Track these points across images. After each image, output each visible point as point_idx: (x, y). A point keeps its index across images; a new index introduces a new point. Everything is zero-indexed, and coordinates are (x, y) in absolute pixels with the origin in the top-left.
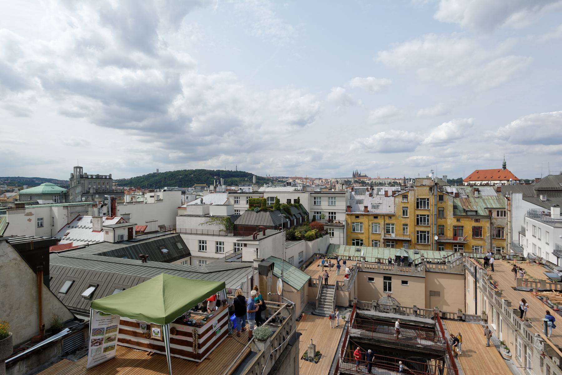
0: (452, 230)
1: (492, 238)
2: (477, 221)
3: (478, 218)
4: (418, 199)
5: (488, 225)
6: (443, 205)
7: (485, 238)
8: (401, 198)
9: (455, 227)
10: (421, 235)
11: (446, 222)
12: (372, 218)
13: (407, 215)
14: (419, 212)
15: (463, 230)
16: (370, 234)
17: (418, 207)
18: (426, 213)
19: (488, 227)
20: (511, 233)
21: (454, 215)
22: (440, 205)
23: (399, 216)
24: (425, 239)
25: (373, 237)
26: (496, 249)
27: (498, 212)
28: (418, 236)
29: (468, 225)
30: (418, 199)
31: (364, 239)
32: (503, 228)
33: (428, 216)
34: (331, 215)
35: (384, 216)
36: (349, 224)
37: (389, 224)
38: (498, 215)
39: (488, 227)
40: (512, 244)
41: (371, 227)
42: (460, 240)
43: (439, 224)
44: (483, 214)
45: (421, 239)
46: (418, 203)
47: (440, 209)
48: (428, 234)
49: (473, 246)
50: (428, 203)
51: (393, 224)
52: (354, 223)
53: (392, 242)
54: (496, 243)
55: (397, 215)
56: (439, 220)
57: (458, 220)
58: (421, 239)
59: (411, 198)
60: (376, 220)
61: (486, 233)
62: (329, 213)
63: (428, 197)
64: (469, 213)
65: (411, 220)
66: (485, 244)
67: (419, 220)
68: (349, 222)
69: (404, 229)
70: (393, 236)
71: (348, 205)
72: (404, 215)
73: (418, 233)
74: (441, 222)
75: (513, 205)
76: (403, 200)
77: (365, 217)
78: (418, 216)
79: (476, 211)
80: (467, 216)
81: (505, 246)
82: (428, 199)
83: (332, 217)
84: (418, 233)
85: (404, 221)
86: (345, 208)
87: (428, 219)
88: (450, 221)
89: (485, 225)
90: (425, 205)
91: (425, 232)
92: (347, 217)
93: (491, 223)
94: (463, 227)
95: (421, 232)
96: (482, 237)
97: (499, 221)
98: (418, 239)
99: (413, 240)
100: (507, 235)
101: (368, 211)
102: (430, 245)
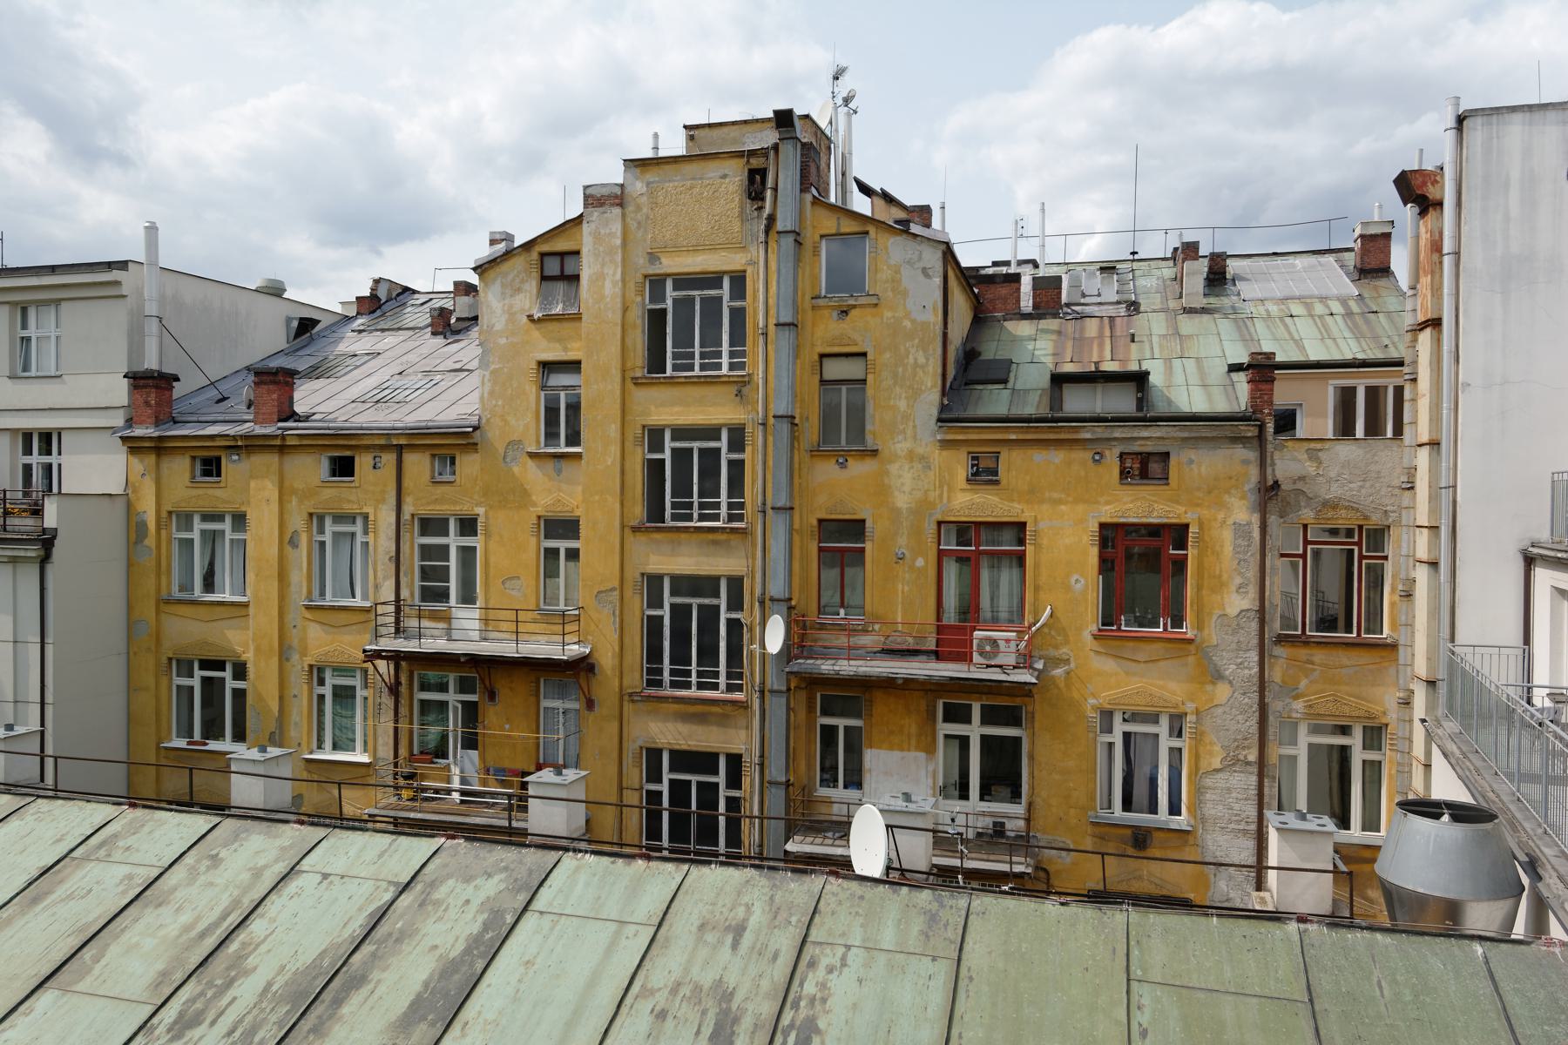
0: (924, 562)
1: (1274, 637)
2: (1144, 468)
3: (1148, 438)
4: (656, 284)
5: (1242, 512)
6: (860, 330)
7: (1213, 634)
8: (532, 285)
9: (965, 531)
10: (680, 613)
11: (882, 491)
12: (315, 469)
13: (574, 439)
14: (671, 408)
15: (1020, 559)
16: (296, 614)
17: (656, 362)
18: (718, 410)
19: (1241, 530)
20: (1445, 566)
21: (945, 418)
22: (826, 331)
23: (514, 444)
24: (708, 654)
25: (319, 642)
26: (1304, 739)
27: (1346, 398)
28: (654, 625)
29: (1067, 515)
30: (656, 284)
31: (249, 656)
32: (1377, 537)
33: (738, 438)
34: (36, 459)
35: (400, 444)
36: (141, 528)
37: (431, 525)
38: (1345, 428)
39: (1241, 530)
40: (1456, 688)
41: (301, 557)
42: (997, 656)
43: (822, 506)
44: (1199, 405)
45: (681, 656)
46: (656, 319)
47: (834, 370)
48: (736, 603)
49: (1107, 715)
50: (738, 316)
51: (468, 526)
52: (186, 520)
53: (465, 686)
54: (1320, 682)
55: (495, 436)
56: (826, 471)
57: (983, 473)
58: (681, 656)
59: (599, 277)
60: (345, 494)
61: (1220, 586)
62: (27, 436)
63: (734, 261)
64: (1077, 401)
65: (598, 486)
66: (1203, 693)
67: (680, 480)
68: (147, 506)
69: (551, 572)
70: (466, 631)
71: (151, 363)
72: (552, 435)
73: (655, 601)
74: (837, 487)
75: (1473, 257)
76: (545, 298)
77: (260, 460)
78: (655, 437)
79: (1139, 379)
80: (1051, 426)
81: (1392, 716)
82: (739, 280)
83: (49, 468)
84: (655, 601)
85: (550, 492)
86: (119, 391)
87: (737, 468)
88: (912, 477)
89: (1214, 506)
90: (711, 338)
91: (703, 585)
92: (138, 465)
93: (1269, 492)
94: (1019, 529)
95: (683, 584)
96: (1187, 630)
97: (1337, 471)
98: (654, 654)
99: (606, 661)
100: (1408, 595)
101: (293, 416)
102: (743, 706)
